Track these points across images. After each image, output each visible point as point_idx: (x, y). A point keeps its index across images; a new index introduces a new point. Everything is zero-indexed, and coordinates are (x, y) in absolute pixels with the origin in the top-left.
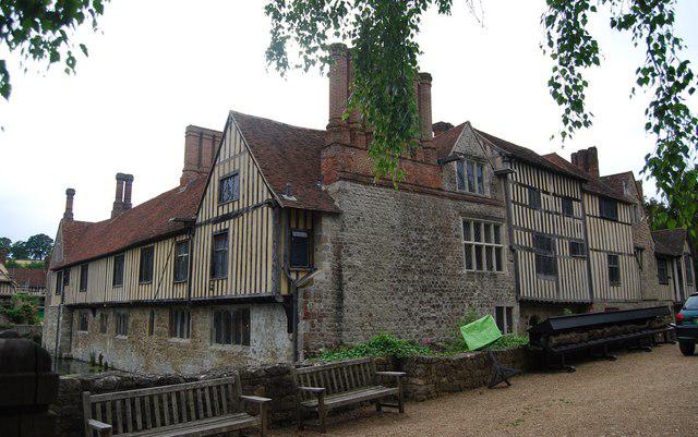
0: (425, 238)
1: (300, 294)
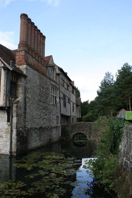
1: (14, 106)
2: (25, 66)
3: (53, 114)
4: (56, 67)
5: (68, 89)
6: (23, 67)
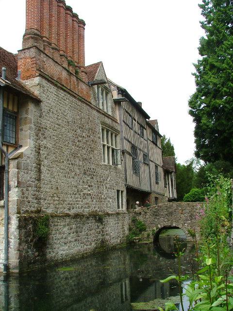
0: (84, 134)
2: (37, 80)
3: (108, 186)
4: (112, 87)
5: (142, 135)
6: (32, 84)
